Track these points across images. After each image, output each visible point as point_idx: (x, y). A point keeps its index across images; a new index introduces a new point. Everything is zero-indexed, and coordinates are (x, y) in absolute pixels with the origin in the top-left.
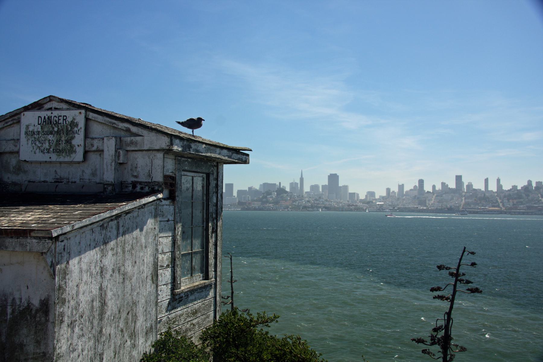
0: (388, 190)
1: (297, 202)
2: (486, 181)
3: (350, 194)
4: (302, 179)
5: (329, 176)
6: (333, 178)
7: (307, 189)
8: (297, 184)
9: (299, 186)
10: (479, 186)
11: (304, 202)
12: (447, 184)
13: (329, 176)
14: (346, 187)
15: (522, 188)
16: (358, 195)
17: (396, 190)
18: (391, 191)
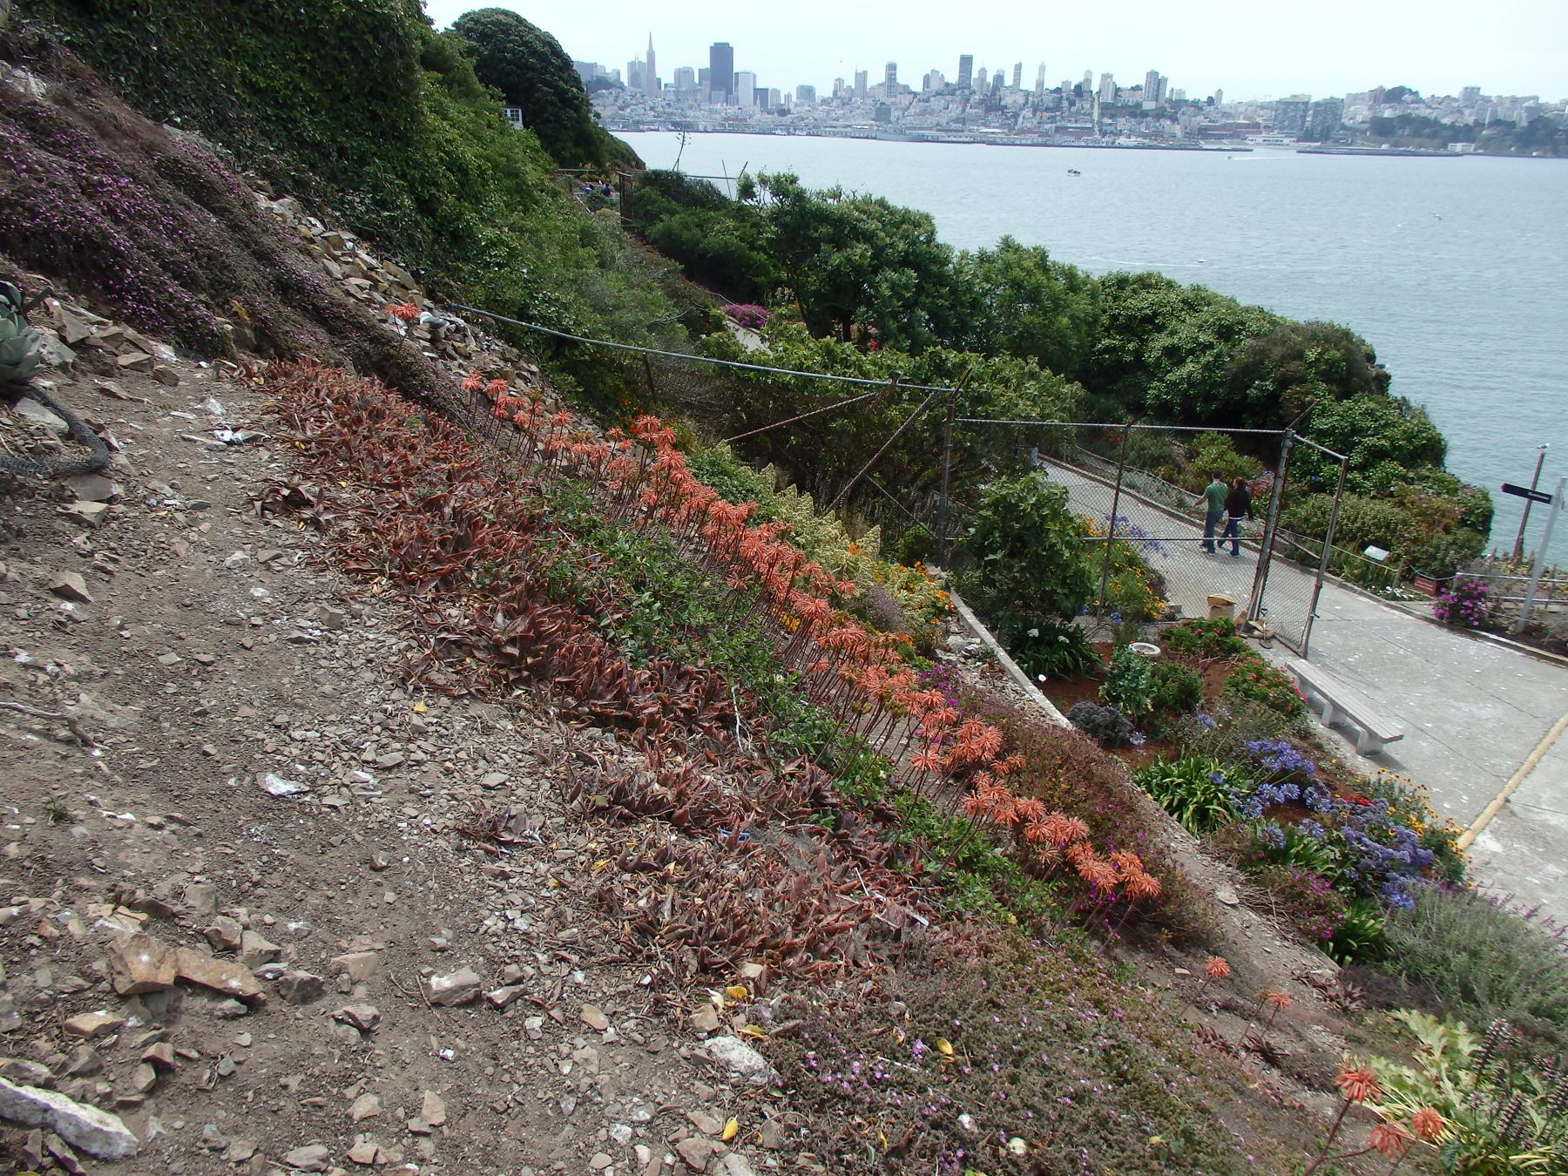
1: (628, 110)
2: (1018, 68)
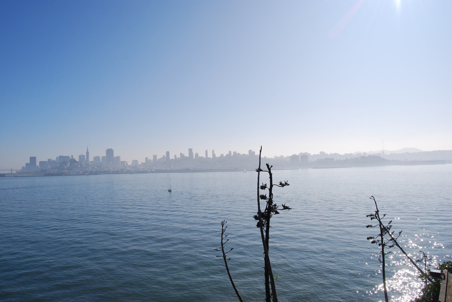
0: (147, 159)
2: (206, 152)
3: (122, 162)
4: (88, 153)
5: (106, 150)
6: (110, 152)
7: (91, 159)
8: (84, 156)
9: (86, 158)
10: (202, 154)
11: (90, 169)
12: (184, 154)
13: (106, 150)
14: (118, 158)
15: (226, 155)
16: (127, 162)
17: (152, 158)
18: (149, 159)
